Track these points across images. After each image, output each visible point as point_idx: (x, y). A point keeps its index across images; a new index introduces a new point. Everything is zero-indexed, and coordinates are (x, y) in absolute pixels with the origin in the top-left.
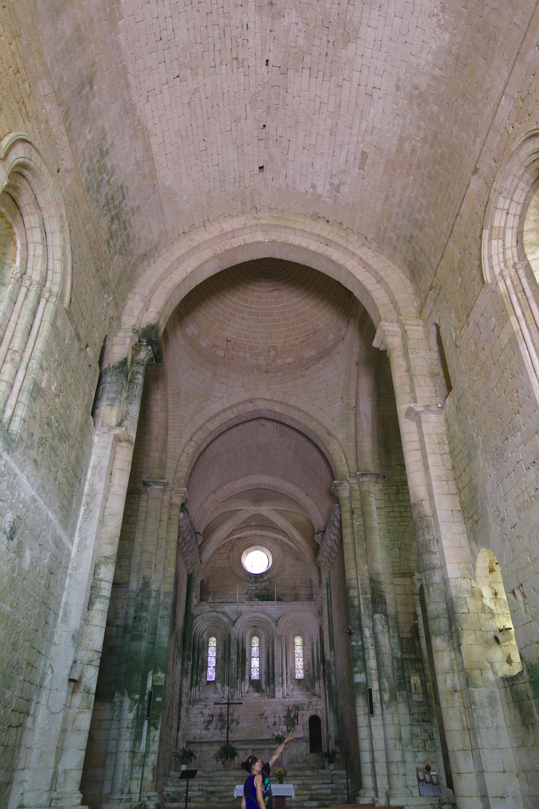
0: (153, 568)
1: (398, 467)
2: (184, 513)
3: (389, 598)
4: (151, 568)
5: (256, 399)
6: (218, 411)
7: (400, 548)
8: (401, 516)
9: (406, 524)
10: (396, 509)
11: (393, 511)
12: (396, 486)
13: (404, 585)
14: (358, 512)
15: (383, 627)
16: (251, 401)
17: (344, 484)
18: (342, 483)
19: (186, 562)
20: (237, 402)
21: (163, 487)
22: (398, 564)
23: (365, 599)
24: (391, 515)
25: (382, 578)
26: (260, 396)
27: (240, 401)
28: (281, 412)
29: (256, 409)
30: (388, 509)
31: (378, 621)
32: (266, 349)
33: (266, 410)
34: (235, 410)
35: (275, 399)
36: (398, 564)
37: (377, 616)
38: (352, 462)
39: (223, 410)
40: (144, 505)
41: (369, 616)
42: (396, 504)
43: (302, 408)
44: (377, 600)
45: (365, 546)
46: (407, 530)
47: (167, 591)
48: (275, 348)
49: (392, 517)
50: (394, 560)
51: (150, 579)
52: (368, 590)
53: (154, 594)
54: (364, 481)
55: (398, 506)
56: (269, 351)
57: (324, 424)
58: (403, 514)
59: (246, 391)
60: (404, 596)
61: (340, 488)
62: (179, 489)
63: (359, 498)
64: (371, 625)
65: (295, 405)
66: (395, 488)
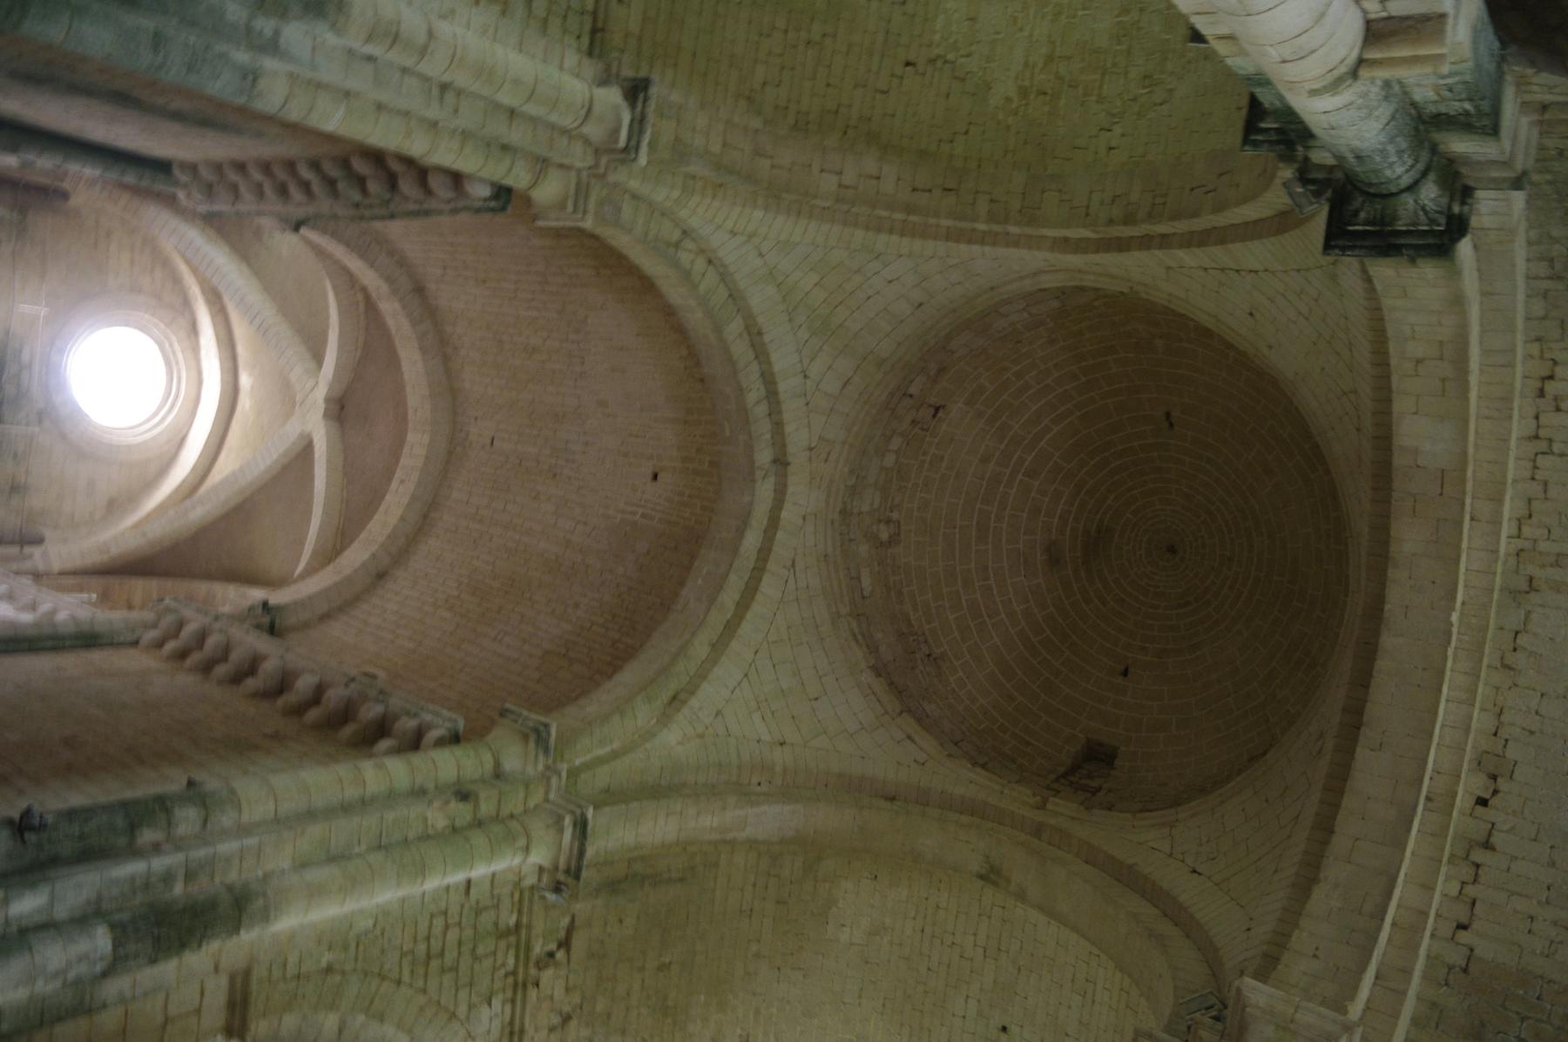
0: (370, 49)
1: (566, 921)
2: (485, 200)
3: (168, 969)
4: (369, 39)
5: (785, 476)
6: (774, 357)
7: (329, 969)
8: (429, 957)
9: (406, 978)
10: (452, 936)
11: (447, 927)
12: (518, 925)
13: (198, 1011)
14: (463, 812)
15: (56, 974)
16: (781, 462)
17: (541, 758)
18: (546, 750)
19: (241, 167)
20: (786, 416)
21: (622, 143)
22: (277, 973)
23: (168, 878)
24: (439, 923)
25: (248, 936)
26: (790, 489)
27: (788, 429)
28: (742, 550)
29: (759, 474)
30: (454, 911)
31: (81, 946)
32: (895, 515)
33: (751, 503)
34: (761, 410)
35: (780, 535)
36: (277, 973)
37: (101, 940)
38: (602, 777)
39: (772, 374)
40: (567, 65)
41: (99, 899)
42: (468, 933)
43: (749, 615)
44: (168, 926)
45: (357, 850)
46: (386, 984)
47: (262, 84)
48: (894, 540)
49: (430, 927)
50: (293, 959)
51: (333, 25)
52: (204, 887)
53: (266, 25)
54: (561, 830)
55: (460, 944)
56: (888, 522)
57: (705, 685)
58: (435, 964)
59: (811, 449)
60: (160, 1019)
61: (532, 744)
62: (593, 200)
63: (505, 812)
64: (61, 913)
65: (759, 597)
66: (513, 920)
